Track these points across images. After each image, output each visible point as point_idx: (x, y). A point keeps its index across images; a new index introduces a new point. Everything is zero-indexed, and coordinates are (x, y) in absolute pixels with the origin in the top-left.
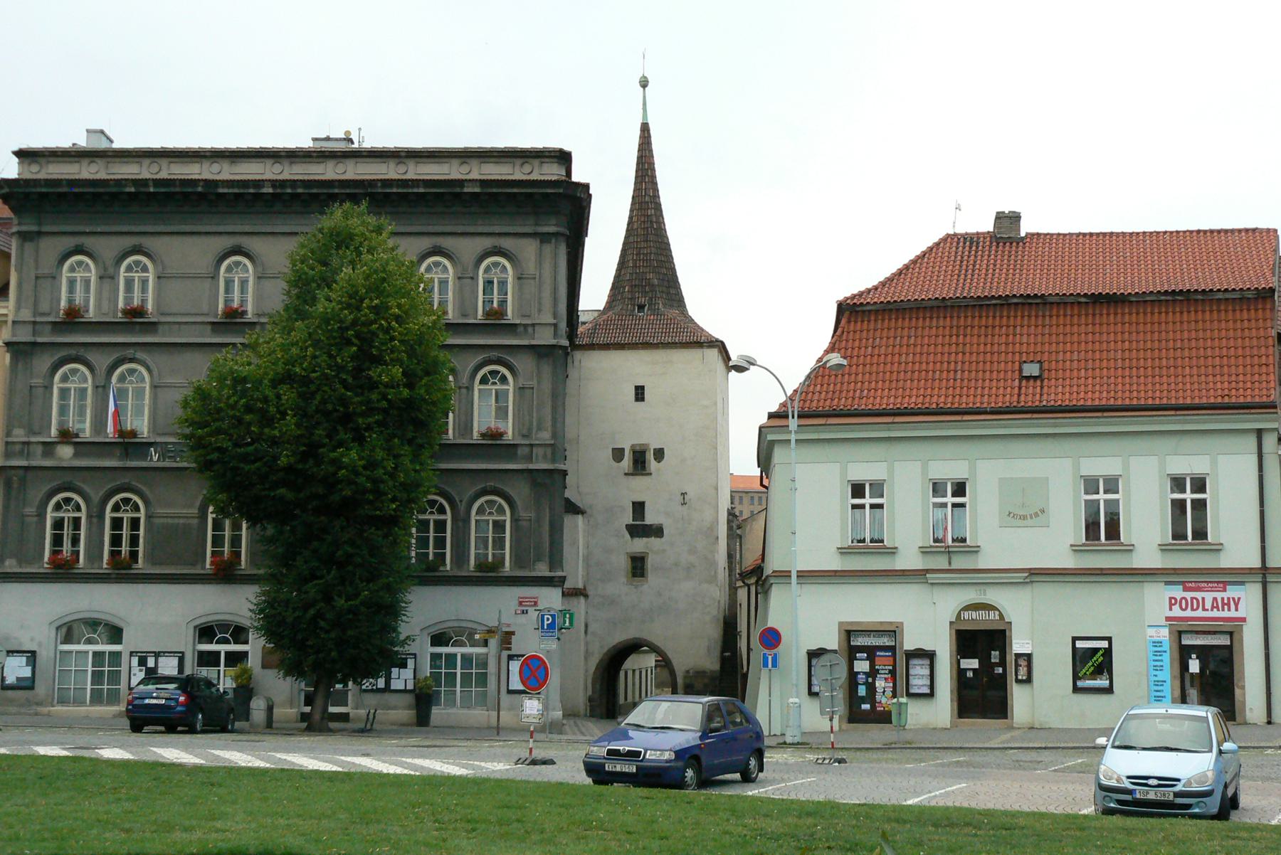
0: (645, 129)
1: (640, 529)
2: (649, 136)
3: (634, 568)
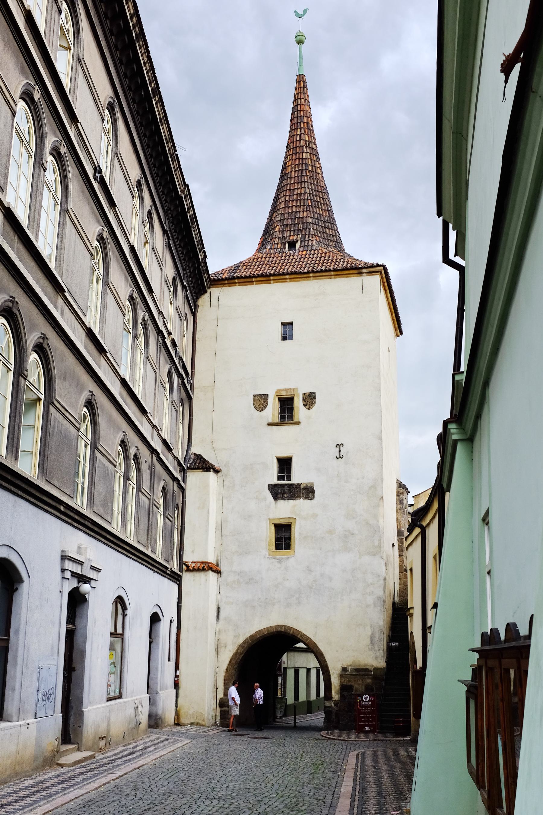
0: (301, 80)
1: (286, 488)
2: (305, 87)
3: (279, 539)
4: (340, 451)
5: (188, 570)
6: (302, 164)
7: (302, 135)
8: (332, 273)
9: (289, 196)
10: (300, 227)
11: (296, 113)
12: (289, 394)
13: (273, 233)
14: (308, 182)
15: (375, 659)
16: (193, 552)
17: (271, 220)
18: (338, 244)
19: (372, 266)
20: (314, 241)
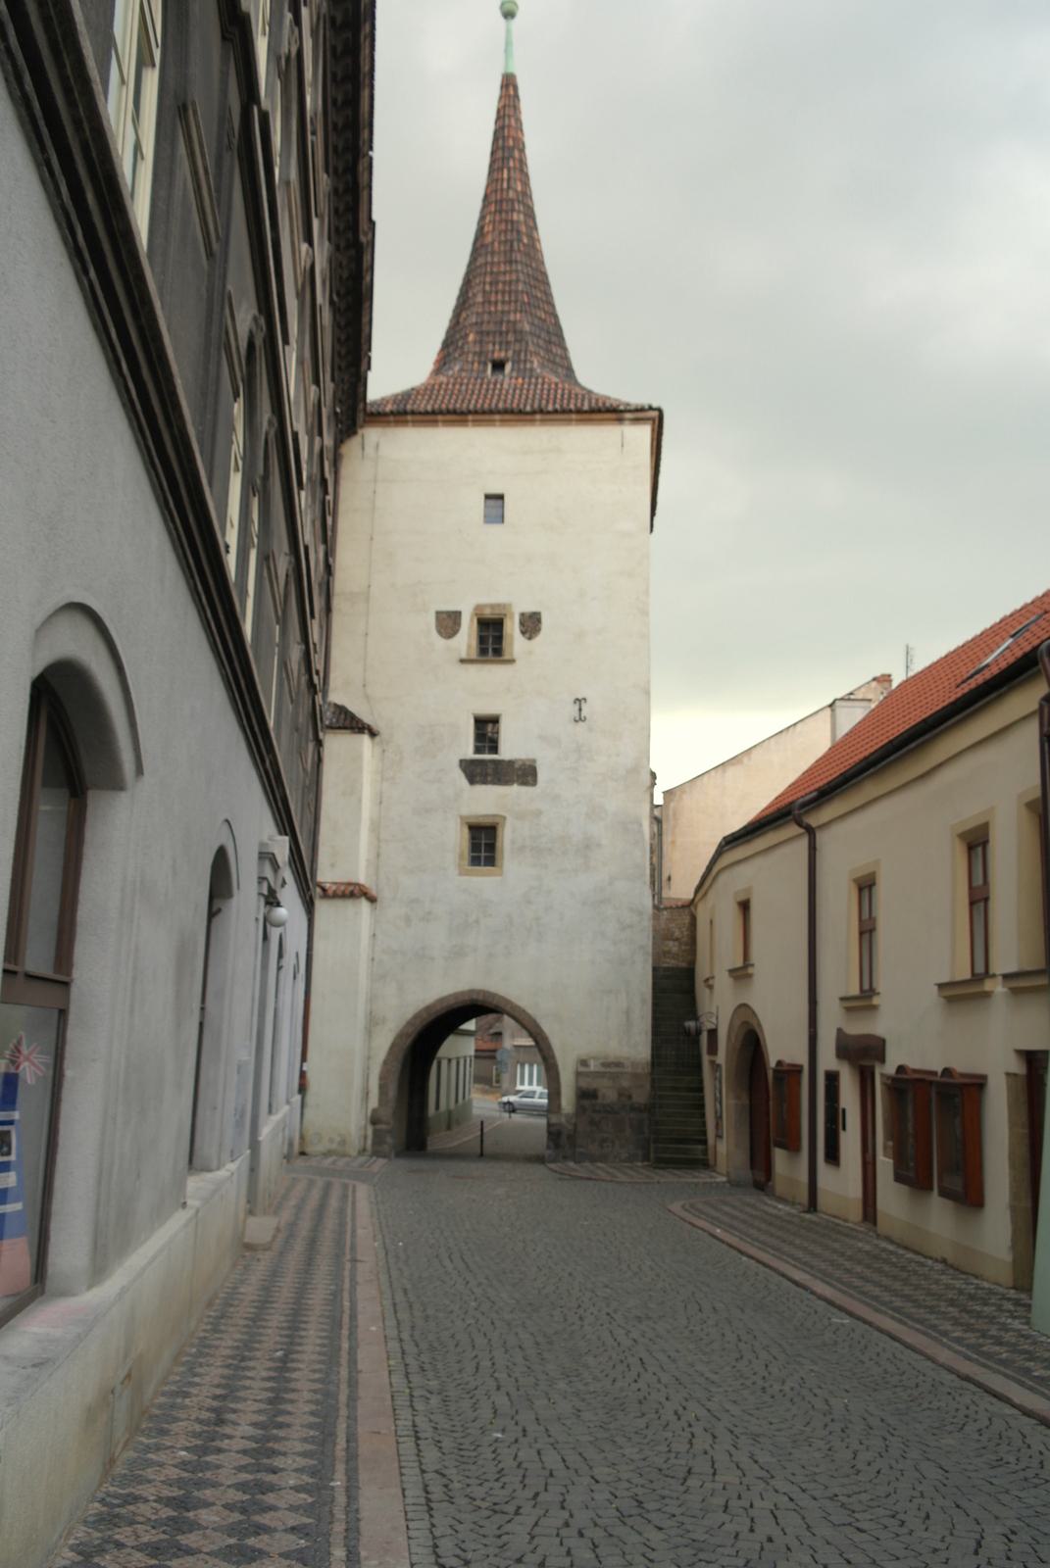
0: (509, 84)
2: (516, 96)
3: (475, 847)
4: (580, 710)
5: (325, 894)
6: (512, 231)
7: (512, 181)
8: (574, 416)
9: (491, 284)
10: (511, 337)
11: (500, 142)
12: (497, 612)
13: (463, 344)
14: (521, 262)
15: (634, 1045)
16: (333, 865)
17: (458, 323)
18: (569, 371)
19: (642, 410)
20: (536, 364)
